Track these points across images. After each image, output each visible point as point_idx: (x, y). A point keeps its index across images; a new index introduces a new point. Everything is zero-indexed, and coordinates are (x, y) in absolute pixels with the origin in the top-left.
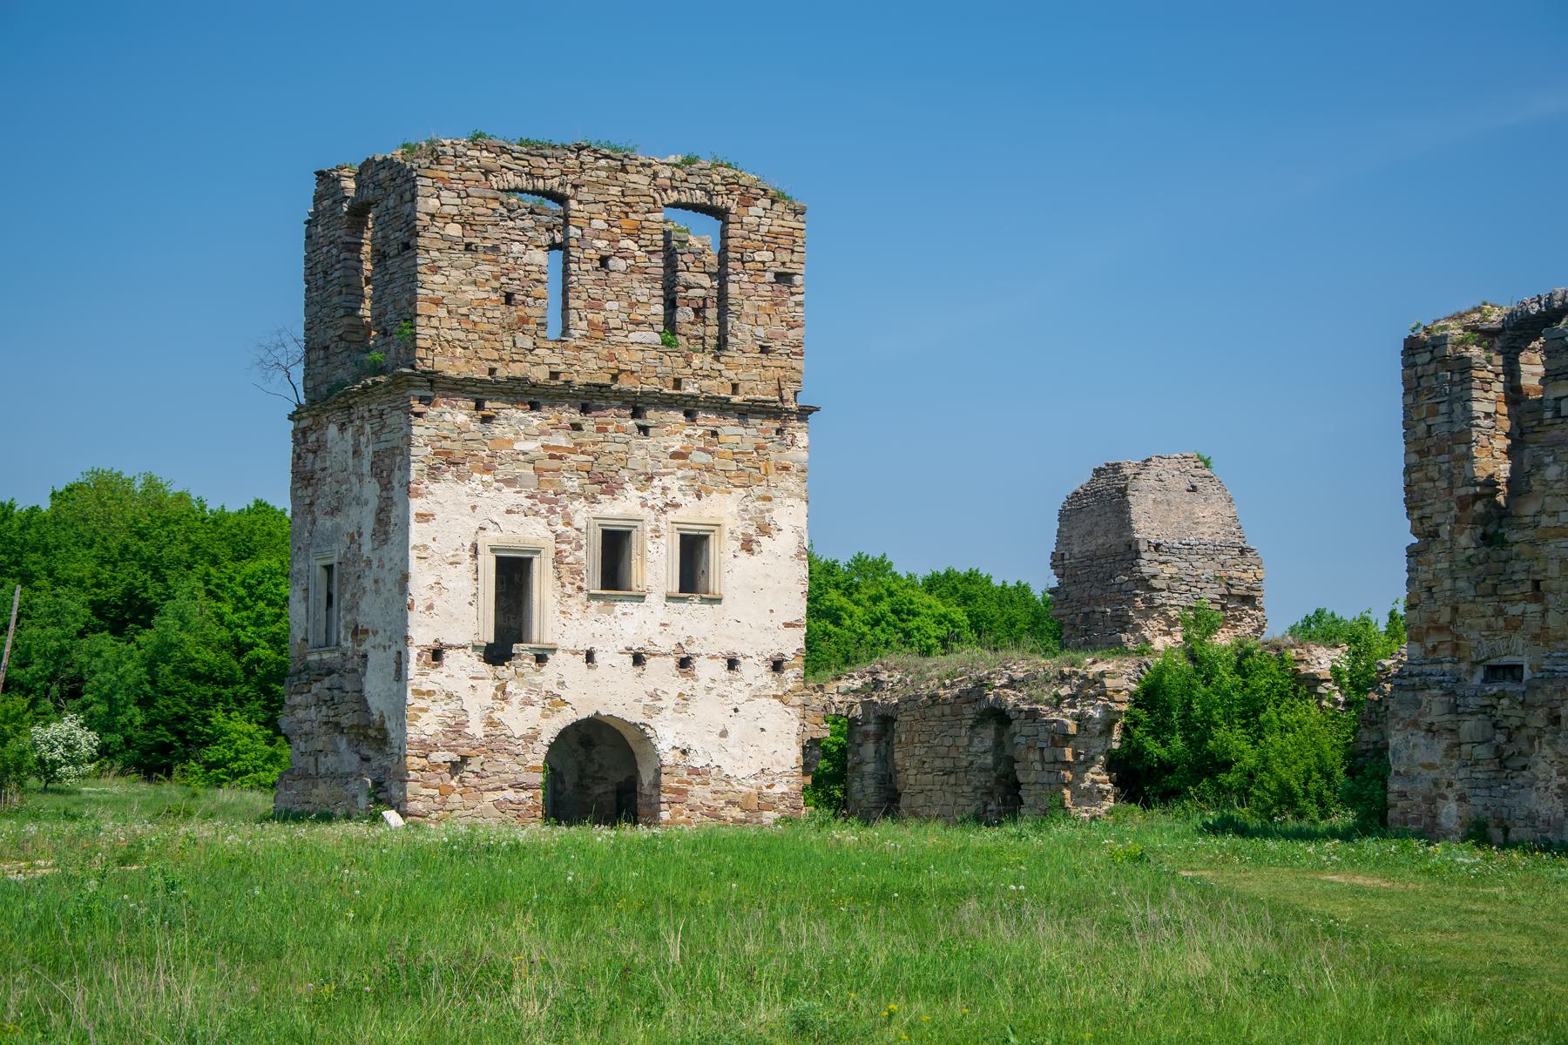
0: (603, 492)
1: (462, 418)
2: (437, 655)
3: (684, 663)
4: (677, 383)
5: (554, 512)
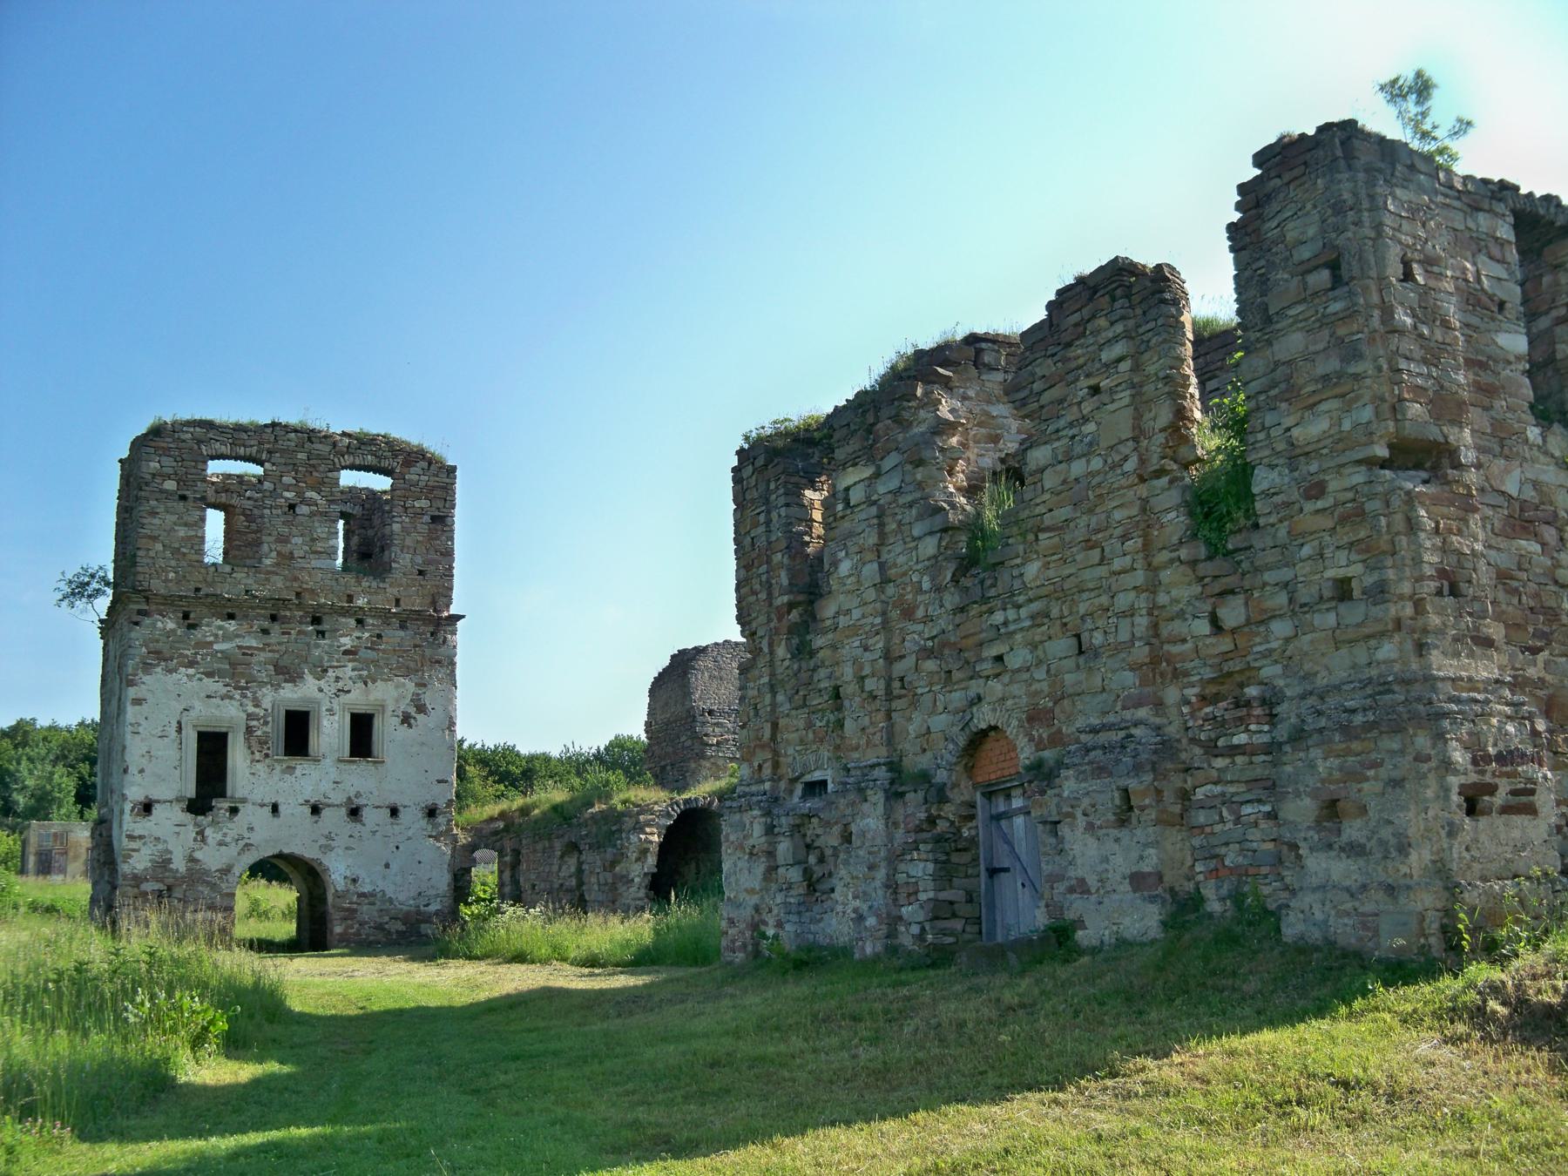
0: (286, 681)
1: (171, 625)
2: (147, 808)
3: (354, 813)
4: (350, 598)
5: (245, 697)
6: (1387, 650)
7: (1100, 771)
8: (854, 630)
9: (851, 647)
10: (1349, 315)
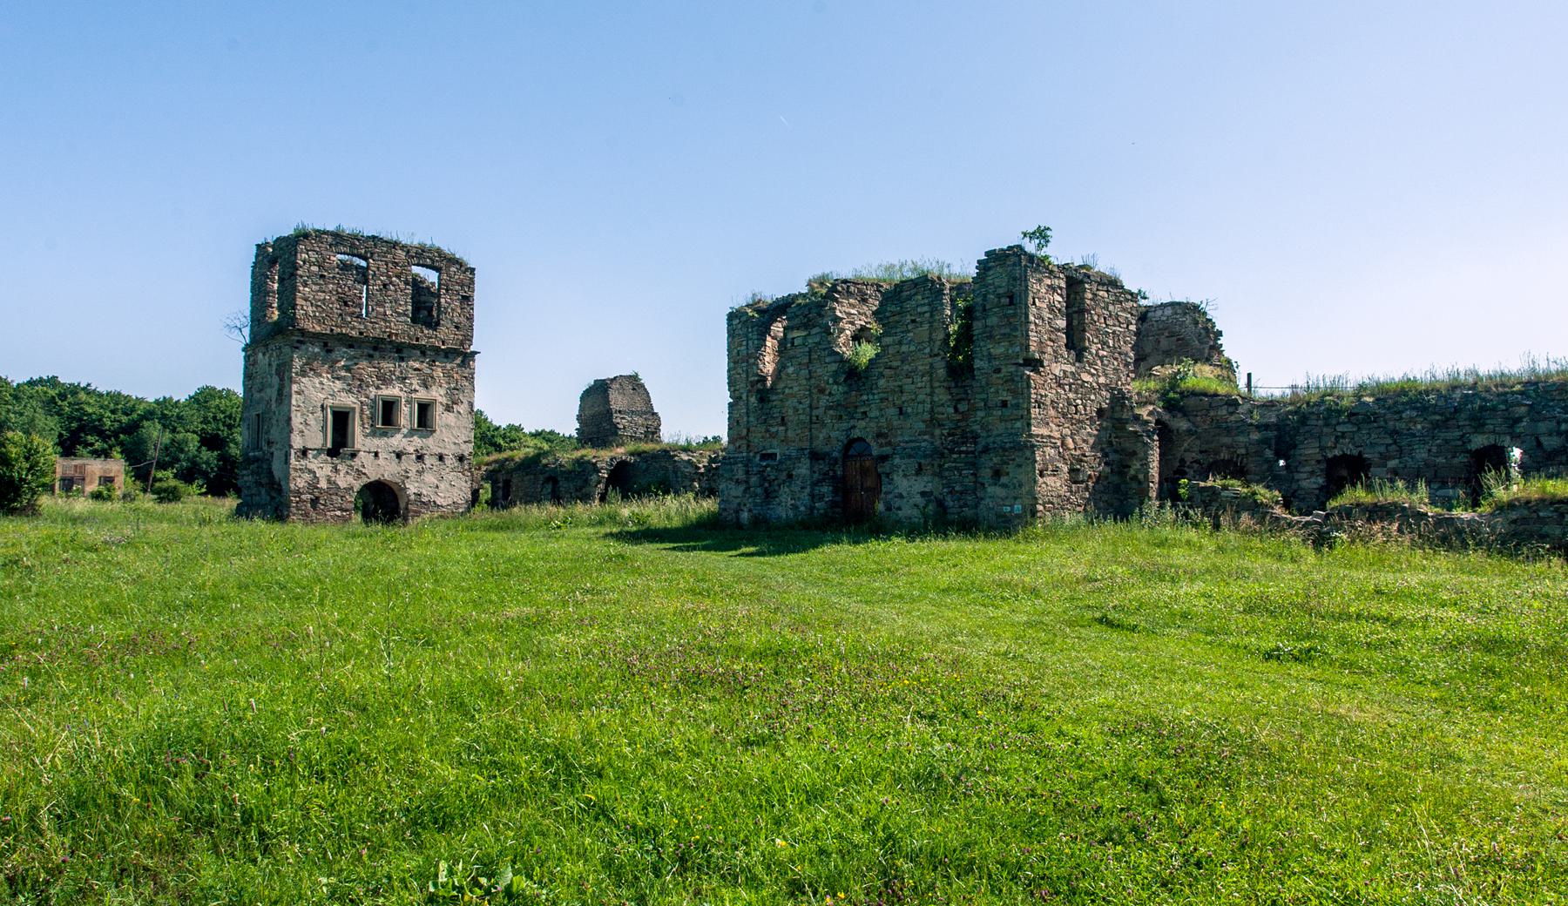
6: (1018, 424)
7: (910, 456)
8: (794, 396)
9: (792, 402)
10: (1015, 315)
